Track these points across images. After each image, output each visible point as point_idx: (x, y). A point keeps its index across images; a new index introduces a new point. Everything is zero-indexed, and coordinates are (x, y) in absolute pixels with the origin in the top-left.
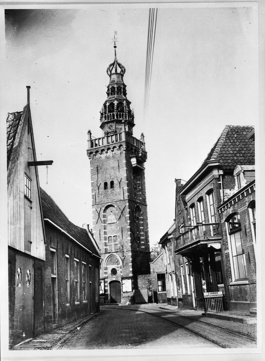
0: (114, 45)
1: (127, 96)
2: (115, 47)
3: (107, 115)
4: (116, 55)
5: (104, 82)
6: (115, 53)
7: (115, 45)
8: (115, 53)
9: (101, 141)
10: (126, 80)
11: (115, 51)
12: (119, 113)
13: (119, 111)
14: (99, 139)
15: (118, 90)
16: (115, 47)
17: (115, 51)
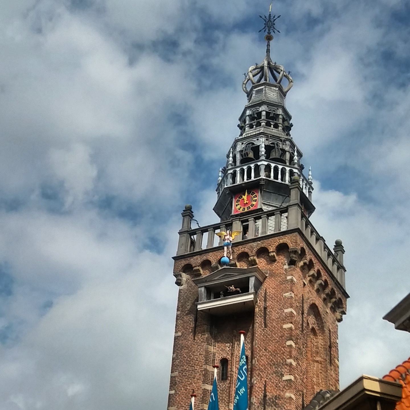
13: (275, 160)
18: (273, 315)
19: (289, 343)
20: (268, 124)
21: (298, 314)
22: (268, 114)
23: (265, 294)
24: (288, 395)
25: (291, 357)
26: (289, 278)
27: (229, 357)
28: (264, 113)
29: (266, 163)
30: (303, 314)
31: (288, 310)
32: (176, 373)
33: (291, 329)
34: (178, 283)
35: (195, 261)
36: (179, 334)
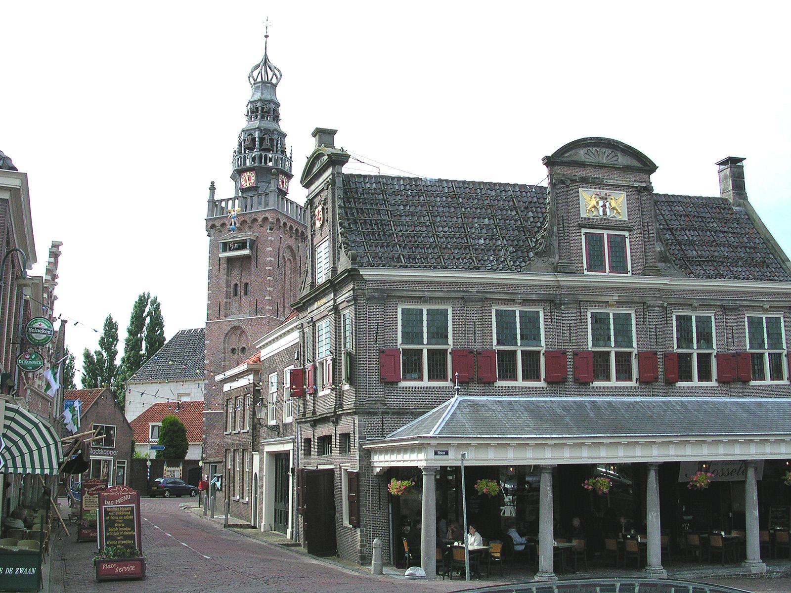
0: (266, 34)
1: (280, 122)
2: (266, 36)
3: (242, 156)
4: (266, 49)
5: (246, 94)
6: (266, 47)
7: (267, 34)
8: (266, 47)
9: (230, 202)
10: (281, 94)
11: (266, 43)
12: (263, 154)
14: (228, 200)
15: (265, 109)
16: (266, 36)
17: (266, 43)
18: (261, 261)
19: (268, 278)
20: (263, 117)
21: (275, 259)
22: (263, 108)
23: (257, 247)
24: (267, 307)
25: (269, 287)
26: (269, 238)
27: (239, 283)
28: (260, 109)
29: (259, 153)
30: (279, 256)
31: (269, 259)
32: (210, 292)
33: (269, 270)
34: (209, 235)
35: (218, 223)
36: (211, 268)
